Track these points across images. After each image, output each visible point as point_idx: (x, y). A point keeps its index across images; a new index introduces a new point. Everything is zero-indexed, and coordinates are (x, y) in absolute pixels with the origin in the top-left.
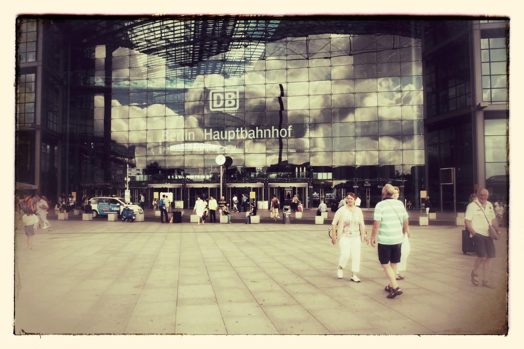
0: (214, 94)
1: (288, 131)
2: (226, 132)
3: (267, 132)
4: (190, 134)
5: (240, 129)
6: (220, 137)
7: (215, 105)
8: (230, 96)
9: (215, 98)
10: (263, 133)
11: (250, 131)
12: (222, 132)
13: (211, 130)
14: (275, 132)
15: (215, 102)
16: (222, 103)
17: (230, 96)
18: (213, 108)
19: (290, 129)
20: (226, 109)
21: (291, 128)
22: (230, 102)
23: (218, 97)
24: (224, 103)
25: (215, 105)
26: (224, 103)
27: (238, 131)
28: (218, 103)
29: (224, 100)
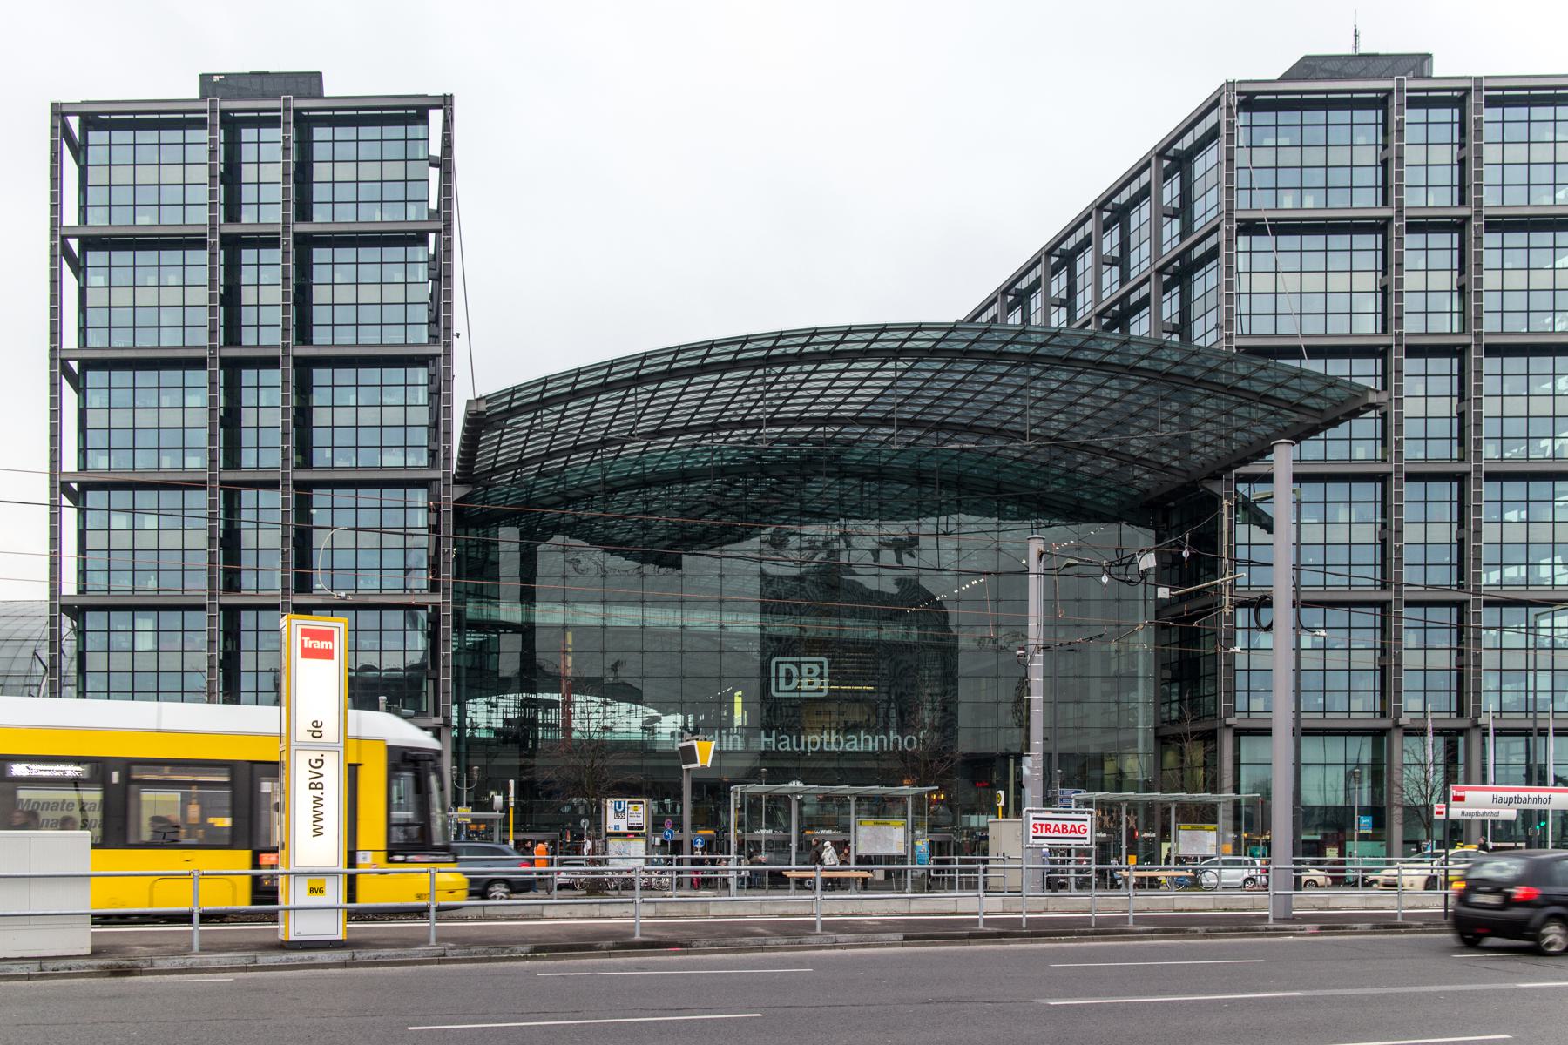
0: (781, 665)
2: (803, 737)
3: (881, 741)
6: (791, 746)
7: (782, 686)
8: (810, 671)
9: (782, 673)
11: (848, 738)
12: (794, 737)
13: (774, 732)
15: (782, 681)
17: (810, 671)
18: (778, 691)
23: (788, 672)
25: (782, 686)
27: (826, 736)
28: (788, 683)
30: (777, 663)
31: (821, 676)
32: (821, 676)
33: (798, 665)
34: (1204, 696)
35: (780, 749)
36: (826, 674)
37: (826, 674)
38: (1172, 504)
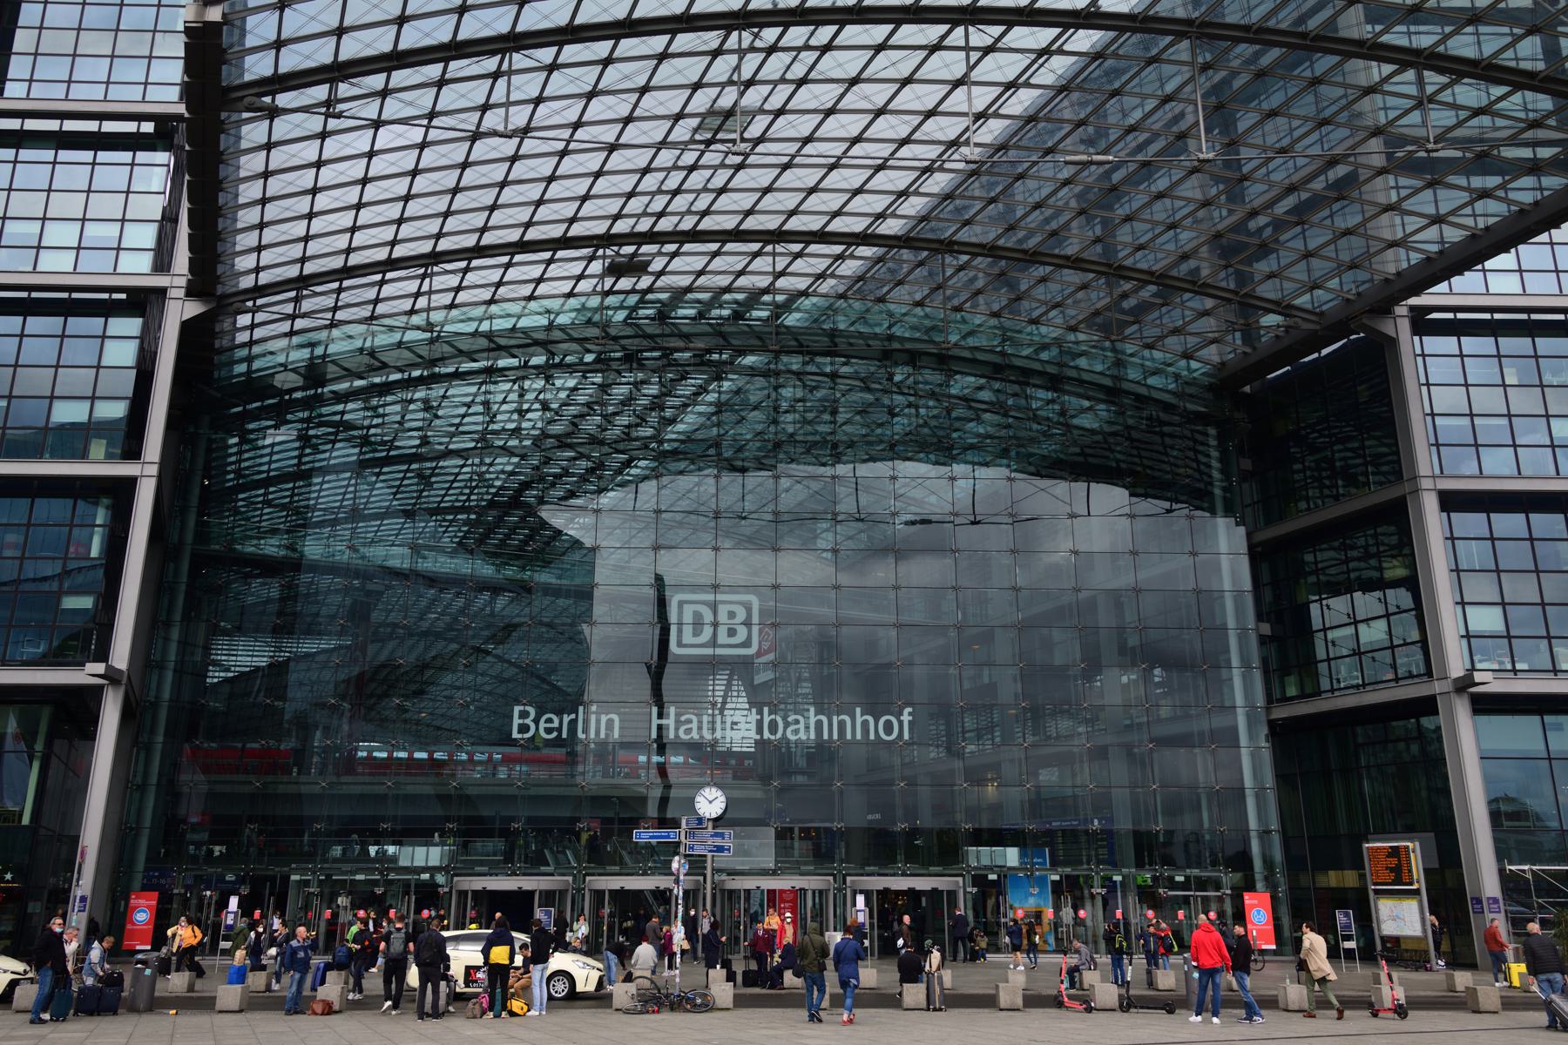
0: (685, 606)
1: (901, 723)
3: (842, 724)
4: (604, 718)
5: (760, 712)
7: (688, 637)
8: (732, 615)
9: (688, 617)
10: (830, 725)
14: (865, 724)
15: (688, 631)
16: (707, 632)
17: (732, 615)
18: (680, 644)
19: (906, 718)
20: (719, 651)
21: (910, 714)
22: (732, 632)
23: (698, 616)
24: (715, 635)
26: (715, 635)
28: (696, 634)
29: (715, 625)
30: (681, 604)
31: (747, 623)
32: (747, 623)
33: (714, 607)
34: (1329, 660)
35: (683, 736)
36: (755, 619)
37: (755, 619)
38: (1247, 389)
